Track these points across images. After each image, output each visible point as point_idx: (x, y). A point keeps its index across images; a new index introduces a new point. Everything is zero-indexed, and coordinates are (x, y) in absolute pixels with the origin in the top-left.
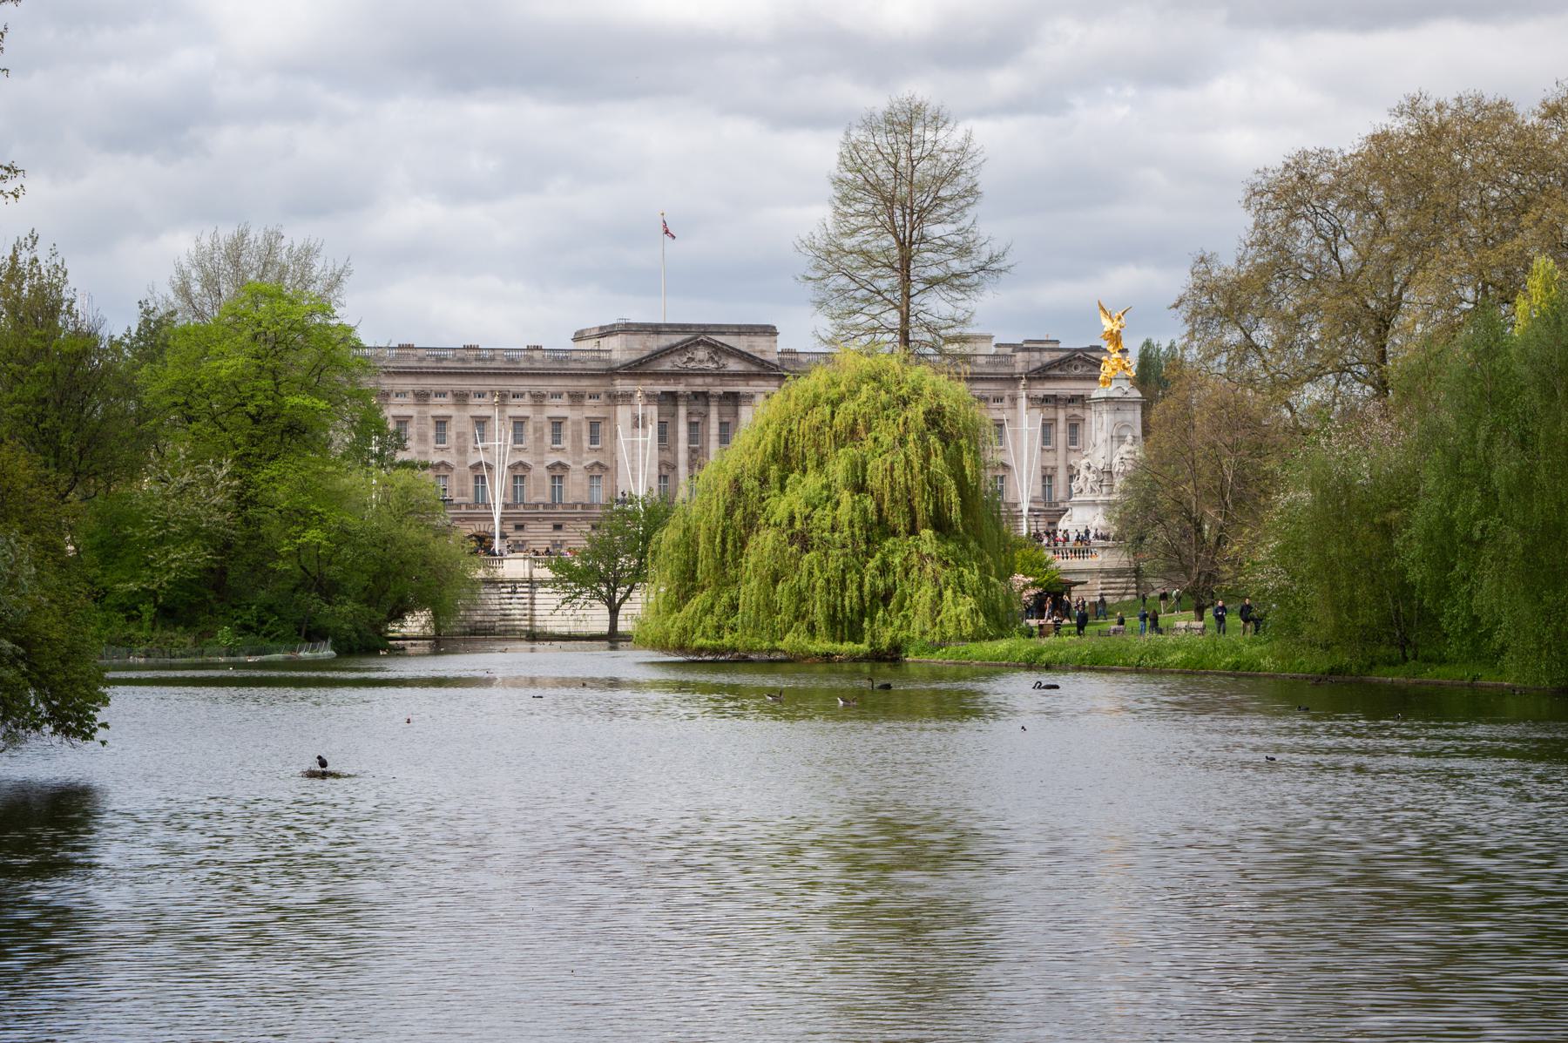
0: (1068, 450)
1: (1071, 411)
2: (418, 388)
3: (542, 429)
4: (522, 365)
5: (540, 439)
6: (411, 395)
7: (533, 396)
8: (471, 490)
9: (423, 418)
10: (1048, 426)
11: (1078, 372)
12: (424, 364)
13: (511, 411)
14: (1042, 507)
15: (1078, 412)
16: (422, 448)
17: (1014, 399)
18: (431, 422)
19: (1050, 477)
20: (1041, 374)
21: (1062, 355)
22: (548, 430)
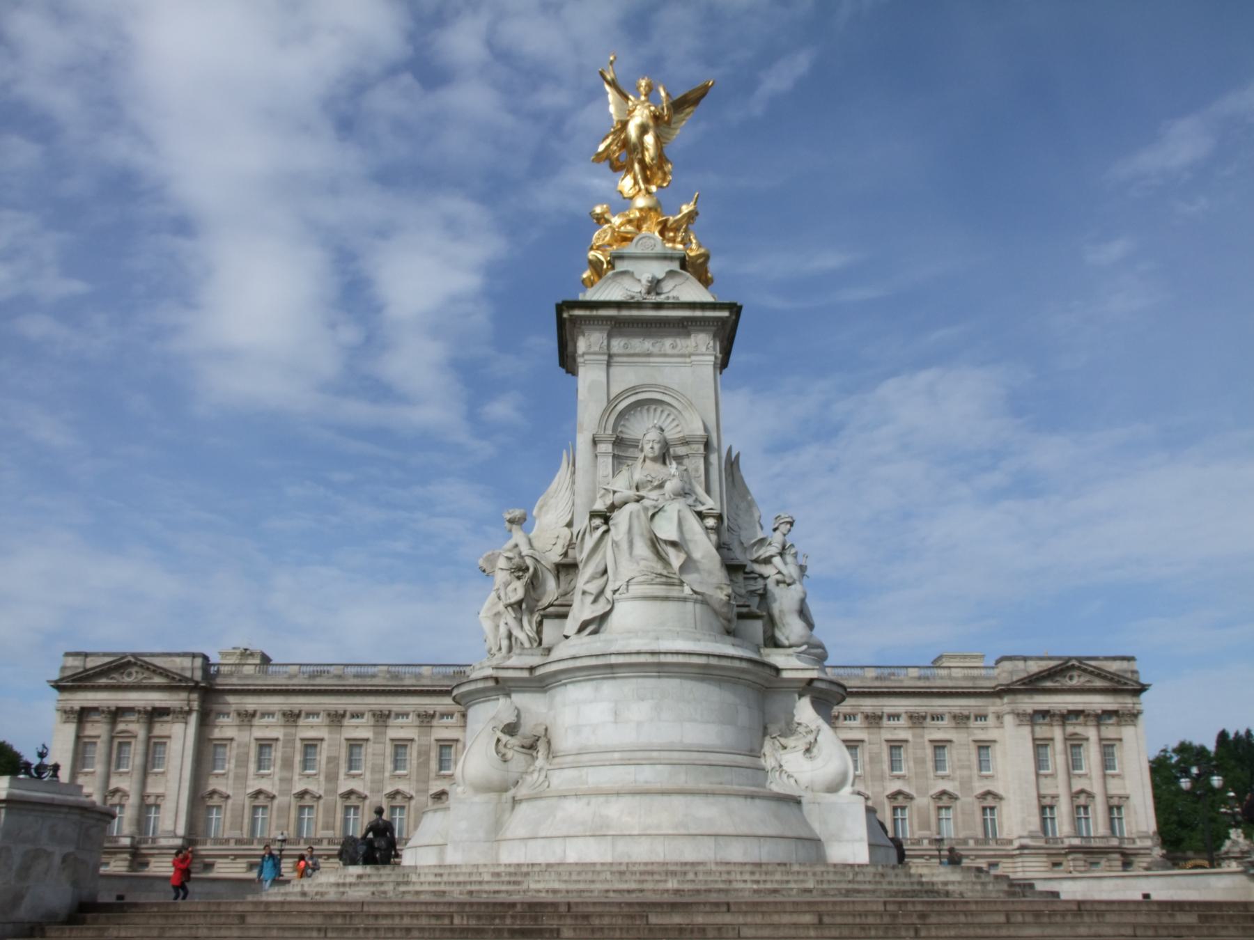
0: (1069, 776)
1: (1070, 729)
2: (286, 708)
3: (427, 753)
4: (407, 682)
5: (424, 764)
6: (278, 716)
7: (419, 716)
8: (338, 823)
9: (289, 742)
10: (1040, 745)
11: (1075, 682)
12: (295, 681)
13: (392, 733)
14: (1041, 843)
15: (1079, 730)
16: (286, 774)
17: (999, 717)
18: (298, 745)
19: (1052, 807)
20: (1032, 685)
21: (1052, 664)
22: (434, 755)
